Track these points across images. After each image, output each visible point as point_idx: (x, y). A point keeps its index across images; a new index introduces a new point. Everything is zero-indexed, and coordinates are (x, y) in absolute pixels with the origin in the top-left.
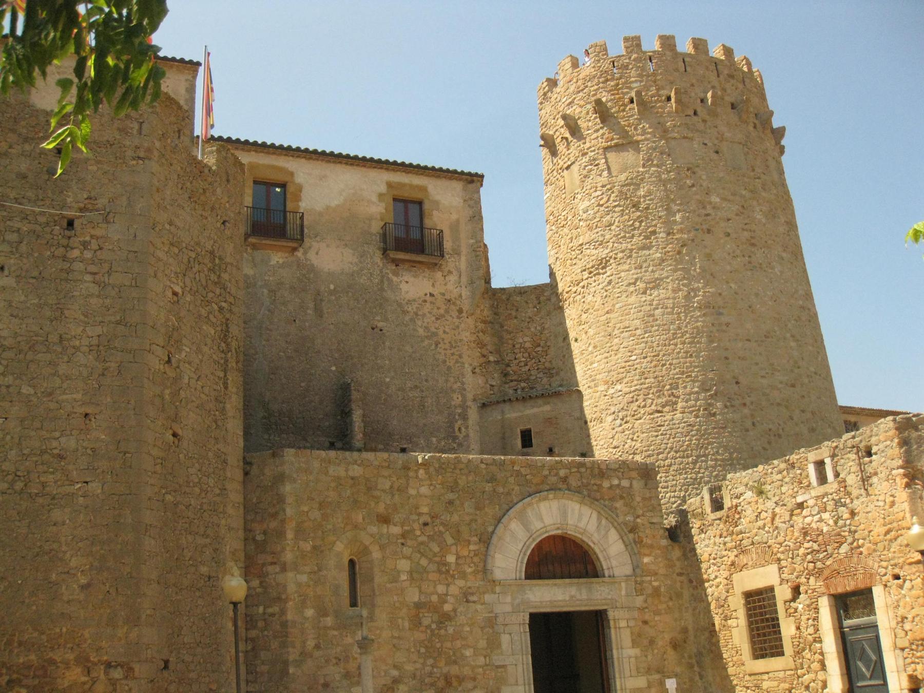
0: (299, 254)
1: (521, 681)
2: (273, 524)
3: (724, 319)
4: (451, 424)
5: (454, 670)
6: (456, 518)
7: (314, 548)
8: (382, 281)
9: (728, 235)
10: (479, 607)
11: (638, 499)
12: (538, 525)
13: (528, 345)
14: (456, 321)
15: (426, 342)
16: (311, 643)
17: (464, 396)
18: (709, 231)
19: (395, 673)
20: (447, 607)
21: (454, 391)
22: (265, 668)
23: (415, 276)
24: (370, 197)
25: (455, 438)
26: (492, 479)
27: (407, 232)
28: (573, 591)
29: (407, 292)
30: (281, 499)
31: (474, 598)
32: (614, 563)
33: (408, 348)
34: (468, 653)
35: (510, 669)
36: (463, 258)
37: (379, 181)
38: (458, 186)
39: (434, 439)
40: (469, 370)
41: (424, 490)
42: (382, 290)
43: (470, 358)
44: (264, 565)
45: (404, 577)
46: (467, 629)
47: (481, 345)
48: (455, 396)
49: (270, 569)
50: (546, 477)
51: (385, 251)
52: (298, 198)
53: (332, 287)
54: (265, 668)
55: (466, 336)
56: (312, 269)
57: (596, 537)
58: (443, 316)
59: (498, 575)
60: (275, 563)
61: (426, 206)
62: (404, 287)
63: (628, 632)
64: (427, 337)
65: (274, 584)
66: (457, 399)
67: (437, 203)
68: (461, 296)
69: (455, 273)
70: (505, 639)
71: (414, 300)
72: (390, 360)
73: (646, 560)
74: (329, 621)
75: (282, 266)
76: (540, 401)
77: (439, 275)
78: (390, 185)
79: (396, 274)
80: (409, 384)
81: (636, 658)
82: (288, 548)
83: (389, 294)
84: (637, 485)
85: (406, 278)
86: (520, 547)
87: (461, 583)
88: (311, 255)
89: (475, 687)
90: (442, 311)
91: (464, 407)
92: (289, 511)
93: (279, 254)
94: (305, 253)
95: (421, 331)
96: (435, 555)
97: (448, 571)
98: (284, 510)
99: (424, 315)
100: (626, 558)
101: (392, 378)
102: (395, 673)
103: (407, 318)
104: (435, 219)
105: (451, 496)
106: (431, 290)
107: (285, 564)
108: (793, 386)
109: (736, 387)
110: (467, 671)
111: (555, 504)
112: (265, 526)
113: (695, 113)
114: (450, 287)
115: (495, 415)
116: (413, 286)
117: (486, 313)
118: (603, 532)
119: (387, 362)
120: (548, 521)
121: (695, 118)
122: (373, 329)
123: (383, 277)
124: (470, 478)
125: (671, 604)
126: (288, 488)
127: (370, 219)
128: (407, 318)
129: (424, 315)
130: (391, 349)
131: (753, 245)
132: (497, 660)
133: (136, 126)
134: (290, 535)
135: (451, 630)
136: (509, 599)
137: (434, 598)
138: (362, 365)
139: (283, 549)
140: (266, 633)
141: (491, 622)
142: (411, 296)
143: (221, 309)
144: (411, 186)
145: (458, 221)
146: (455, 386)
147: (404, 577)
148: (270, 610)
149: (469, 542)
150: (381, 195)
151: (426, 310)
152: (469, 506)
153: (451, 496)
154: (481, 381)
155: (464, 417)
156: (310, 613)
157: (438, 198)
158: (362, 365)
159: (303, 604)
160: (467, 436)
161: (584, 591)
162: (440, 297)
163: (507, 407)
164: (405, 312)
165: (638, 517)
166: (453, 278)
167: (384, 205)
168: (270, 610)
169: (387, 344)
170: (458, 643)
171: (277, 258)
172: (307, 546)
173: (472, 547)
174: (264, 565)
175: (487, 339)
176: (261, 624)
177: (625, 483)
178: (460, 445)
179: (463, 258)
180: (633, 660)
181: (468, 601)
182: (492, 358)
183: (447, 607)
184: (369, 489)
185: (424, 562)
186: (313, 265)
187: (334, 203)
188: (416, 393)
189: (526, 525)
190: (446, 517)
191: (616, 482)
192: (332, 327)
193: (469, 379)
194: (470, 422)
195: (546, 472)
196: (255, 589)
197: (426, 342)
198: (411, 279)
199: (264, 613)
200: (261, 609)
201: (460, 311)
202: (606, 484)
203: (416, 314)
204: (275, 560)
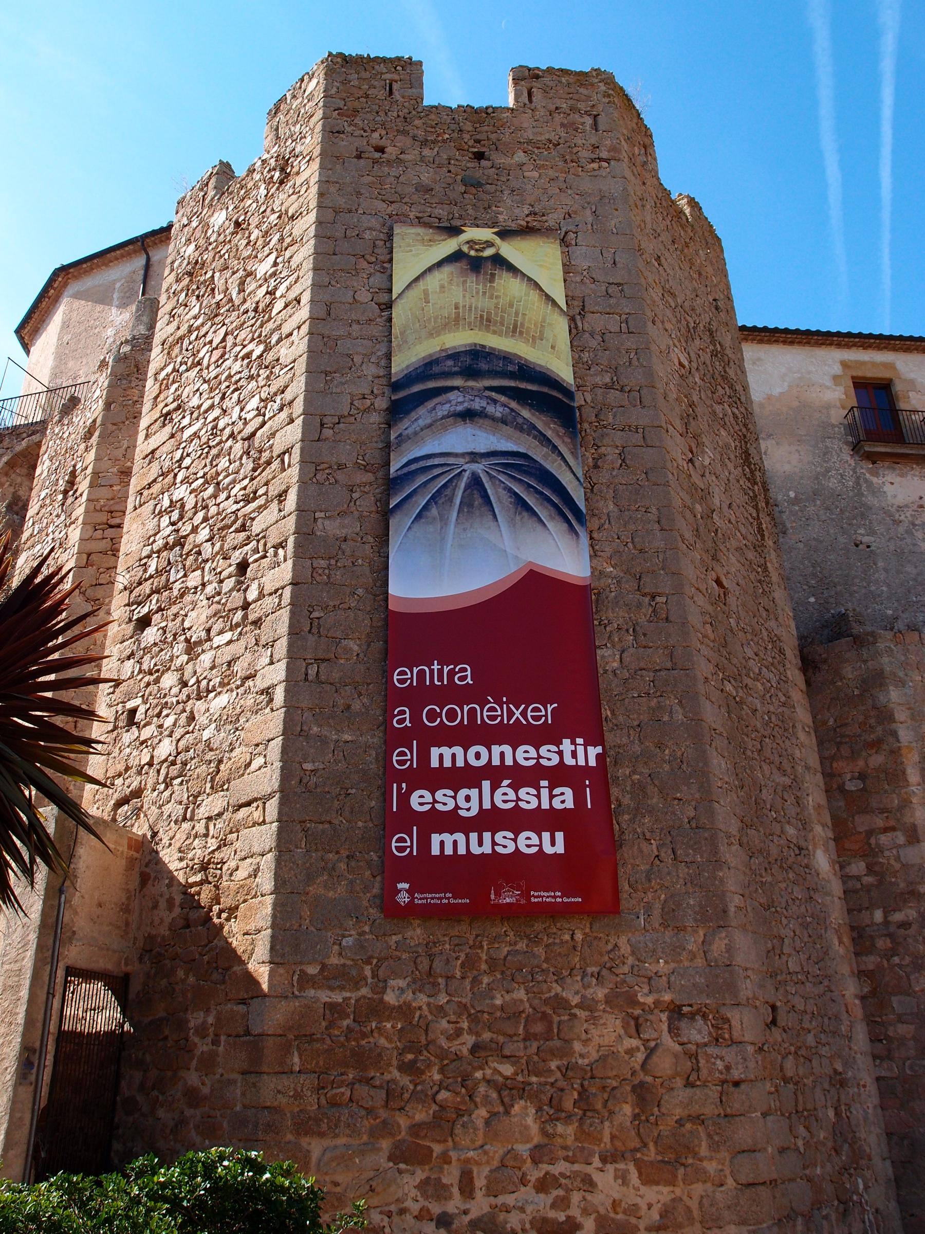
2: (877, 760)
22: (903, 1029)
23: (902, 476)
29: (895, 496)
30: (886, 716)
33: (909, 569)
37: (827, 364)
44: (870, 833)
49: (884, 839)
53: (792, 494)
54: (903, 1029)
60: (893, 829)
61: (898, 387)
62: (887, 488)
65: (897, 866)
67: (912, 382)
71: (907, 506)
72: (888, 586)
78: (845, 365)
79: (876, 475)
82: (914, 800)
83: (870, 500)
85: (889, 478)
92: (905, 735)
98: (894, 734)
103: (901, 529)
104: (913, 402)
107: (914, 828)
112: (861, 763)
119: (884, 588)
122: (857, 546)
123: (858, 478)
126: (894, 695)
127: (828, 407)
128: (901, 529)
130: (886, 570)
133: (589, 121)
138: (851, 595)
139: (906, 803)
140: (896, 959)
142: (901, 500)
144: (874, 364)
148: (898, 917)
150: (836, 379)
157: (912, 376)
158: (851, 595)
164: (898, 522)
167: (842, 389)
168: (898, 917)
169: (880, 564)
174: (870, 833)
176: (882, 943)
187: (776, 391)
192: (801, 545)
196: (858, 878)
198: (897, 480)
199: (886, 923)
200: (878, 915)
203: (914, 525)
204: (892, 823)
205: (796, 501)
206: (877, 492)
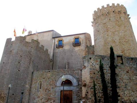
0: (63, 48)
5: (49, 97)
7: (36, 82)
16: (34, 93)
19: (43, 97)
20: (50, 89)
24: (72, 39)
28: (67, 87)
36: (84, 44)
38: (83, 35)
42: (73, 50)
45: (45, 85)
52: (63, 41)
56: (65, 49)
57: (72, 80)
67: (80, 38)
74: (36, 90)
75: (61, 50)
77: (80, 47)
78: (74, 37)
95: (78, 54)
100: (76, 83)
102: (43, 97)
116: (77, 49)
127: (72, 42)
131: (116, 32)
134: (34, 80)
137: (48, 88)
143: (30, 57)
147: (45, 85)
150: (73, 39)
152: (54, 76)
156: (34, 89)
159: (34, 88)
161: (69, 87)
171: (61, 49)
172: (35, 82)
175: (87, 54)
184: (43, 75)
185: (48, 83)
188: (77, 62)
190: (51, 78)
191: (76, 72)
202: (74, 72)
206: (74, 49)
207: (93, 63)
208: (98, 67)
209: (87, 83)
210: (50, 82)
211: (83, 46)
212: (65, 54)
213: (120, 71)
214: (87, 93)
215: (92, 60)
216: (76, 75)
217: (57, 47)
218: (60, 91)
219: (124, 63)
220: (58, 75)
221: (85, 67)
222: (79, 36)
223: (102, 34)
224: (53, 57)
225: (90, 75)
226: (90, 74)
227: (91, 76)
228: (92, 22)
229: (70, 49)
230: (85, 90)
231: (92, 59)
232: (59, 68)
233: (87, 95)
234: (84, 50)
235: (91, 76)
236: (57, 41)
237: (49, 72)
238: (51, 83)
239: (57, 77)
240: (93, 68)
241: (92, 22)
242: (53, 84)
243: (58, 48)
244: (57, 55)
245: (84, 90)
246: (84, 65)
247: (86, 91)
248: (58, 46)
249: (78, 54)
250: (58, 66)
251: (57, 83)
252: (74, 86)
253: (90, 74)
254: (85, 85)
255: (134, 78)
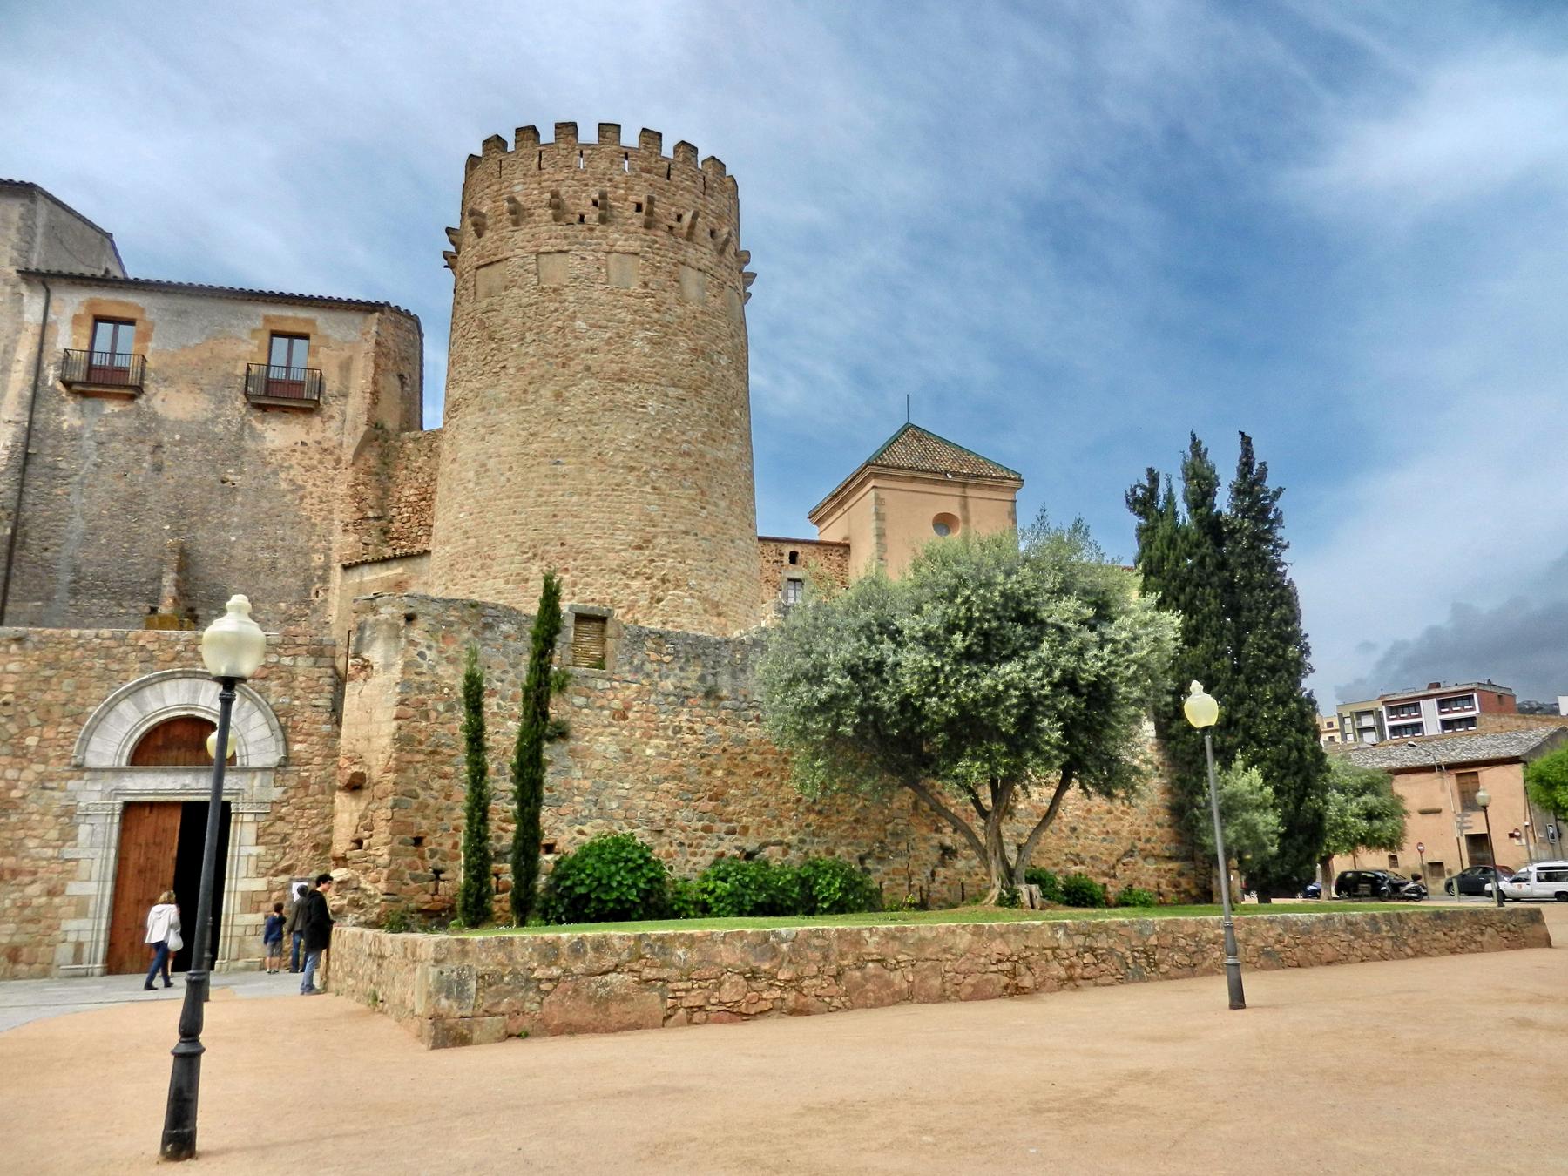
0: (141, 401)
1: (95, 876)
3: (561, 469)
4: (307, 589)
6: (48, 697)
8: (242, 429)
9: (588, 369)
10: (57, 794)
11: (301, 679)
12: (157, 706)
13: (412, 499)
14: (331, 473)
15: (289, 497)
17: (327, 556)
18: (564, 365)
20: (15, 794)
21: (315, 551)
25: (308, 603)
26: (108, 655)
27: (288, 374)
31: (54, 785)
32: (251, 750)
34: (31, 843)
35: (84, 864)
39: (283, 605)
40: (340, 528)
41: (12, 667)
42: (241, 438)
43: (344, 512)
46: (36, 817)
47: (358, 498)
48: (315, 556)
50: (179, 653)
51: (246, 394)
53: (177, 437)
55: (342, 489)
56: (155, 417)
58: (314, 467)
59: (92, 761)
62: (269, 435)
63: (254, 827)
64: (292, 491)
66: (318, 560)
68: (341, 444)
69: (338, 417)
70: (84, 831)
73: (297, 747)
75: (118, 415)
76: (395, 564)
77: (317, 420)
78: (267, 319)
80: (260, 543)
81: (258, 856)
83: (249, 444)
84: (303, 662)
85: (273, 425)
86: (127, 728)
87: (41, 768)
88: (157, 403)
89: (33, 882)
90: (315, 462)
91: (326, 567)
93: (116, 402)
94: (149, 400)
95: (284, 485)
96: (11, 737)
97: (25, 755)
99: (291, 467)
101: (239, 538)
103: (268, 470)
105: (48, 673)
106: (304, 438)
108: (640, 548)
109: (559, 549)
110: (27, 864)
111: (184, 683)
113: (582, 219)
114: (329, 434)
115: (354, 577)
116: (278, 434)
117: (372, 462)
118: (244, 715)
120: (171, 700)
121: (580, 227)
124: (77, 654)
125: (319, 797)
127: (237, 358)
129: (291, 467)
130: (243, 505)
132: (68, 852)
135: (14, 819)
136: (99, 787)
141: (69, 812)
145: (351, 358)
146: (319, 545)
149: (60, 724)
151: (294, 462)
152: (68, 684)
153: (48, 673)
154: (352, 538)
155: (324, 579)
160: (326, 601)
162: (314, 446)
163: (366, 569)
165: (297, 698)
166: (334, 424)
169: (239, 499)
170: (21, 833)
171: (111, 407)
173: (61, 729)
177: (287, 661)
178: (315, 611)
179: (351, 400)
180: (253, 859)
181: (44, 788)
182: (371, 514)
183: (15, 794)
186: (155, 413)
189: (139, 707)
193: (338, 538)
194: (331, 585)
195: (178, 648)
197: (289, 497)
201: (338, 461)
205: (181, 442)
206: (257, 437)
207: (420, 649)
208: (453, 679)
209: (375, 774)
210: (25, 730)
211: (343, 413)
212: (158, 468)
213: (580, 708)
214: (367, 834)
215: (417, 633)
216: (273, 684)
217: (68, 385)
218: (118, 809)
219: (609, 662)
220: (105, 676)
221: (366, 666)
222: (311, 322)
223: (521, 369)
224: (23, 470)
225: (395, 724)
226: (397, 718)
227: (404, 731)
228: (449, 231)
229: (213, 421)
230: (356, 815)
231: (422, 623)
232: (74, 593)
233: (365, 842)
234: (348, 455)
235: (399, 728)
236: (76, 320)
237: (14, 648)
238: (31, 741)
239: (96, 693)
240: (417, 678)
241: (449, 231)
242: (51, 753)
243: (85, 395)
244: (63, 465)
245: (346, 816)
246: (366, 655)
247: (362, 817)
248: (79, 375)
249: (284, 485)
250: (76, 570)
251: (96, 743)
252: (245, 770)
253: (397, 718)
254: (356, 785)
255: (649, 752)
